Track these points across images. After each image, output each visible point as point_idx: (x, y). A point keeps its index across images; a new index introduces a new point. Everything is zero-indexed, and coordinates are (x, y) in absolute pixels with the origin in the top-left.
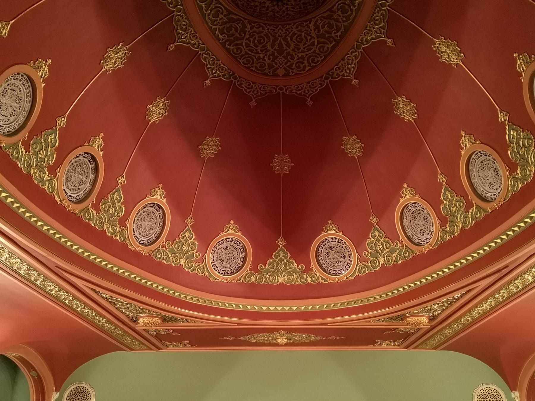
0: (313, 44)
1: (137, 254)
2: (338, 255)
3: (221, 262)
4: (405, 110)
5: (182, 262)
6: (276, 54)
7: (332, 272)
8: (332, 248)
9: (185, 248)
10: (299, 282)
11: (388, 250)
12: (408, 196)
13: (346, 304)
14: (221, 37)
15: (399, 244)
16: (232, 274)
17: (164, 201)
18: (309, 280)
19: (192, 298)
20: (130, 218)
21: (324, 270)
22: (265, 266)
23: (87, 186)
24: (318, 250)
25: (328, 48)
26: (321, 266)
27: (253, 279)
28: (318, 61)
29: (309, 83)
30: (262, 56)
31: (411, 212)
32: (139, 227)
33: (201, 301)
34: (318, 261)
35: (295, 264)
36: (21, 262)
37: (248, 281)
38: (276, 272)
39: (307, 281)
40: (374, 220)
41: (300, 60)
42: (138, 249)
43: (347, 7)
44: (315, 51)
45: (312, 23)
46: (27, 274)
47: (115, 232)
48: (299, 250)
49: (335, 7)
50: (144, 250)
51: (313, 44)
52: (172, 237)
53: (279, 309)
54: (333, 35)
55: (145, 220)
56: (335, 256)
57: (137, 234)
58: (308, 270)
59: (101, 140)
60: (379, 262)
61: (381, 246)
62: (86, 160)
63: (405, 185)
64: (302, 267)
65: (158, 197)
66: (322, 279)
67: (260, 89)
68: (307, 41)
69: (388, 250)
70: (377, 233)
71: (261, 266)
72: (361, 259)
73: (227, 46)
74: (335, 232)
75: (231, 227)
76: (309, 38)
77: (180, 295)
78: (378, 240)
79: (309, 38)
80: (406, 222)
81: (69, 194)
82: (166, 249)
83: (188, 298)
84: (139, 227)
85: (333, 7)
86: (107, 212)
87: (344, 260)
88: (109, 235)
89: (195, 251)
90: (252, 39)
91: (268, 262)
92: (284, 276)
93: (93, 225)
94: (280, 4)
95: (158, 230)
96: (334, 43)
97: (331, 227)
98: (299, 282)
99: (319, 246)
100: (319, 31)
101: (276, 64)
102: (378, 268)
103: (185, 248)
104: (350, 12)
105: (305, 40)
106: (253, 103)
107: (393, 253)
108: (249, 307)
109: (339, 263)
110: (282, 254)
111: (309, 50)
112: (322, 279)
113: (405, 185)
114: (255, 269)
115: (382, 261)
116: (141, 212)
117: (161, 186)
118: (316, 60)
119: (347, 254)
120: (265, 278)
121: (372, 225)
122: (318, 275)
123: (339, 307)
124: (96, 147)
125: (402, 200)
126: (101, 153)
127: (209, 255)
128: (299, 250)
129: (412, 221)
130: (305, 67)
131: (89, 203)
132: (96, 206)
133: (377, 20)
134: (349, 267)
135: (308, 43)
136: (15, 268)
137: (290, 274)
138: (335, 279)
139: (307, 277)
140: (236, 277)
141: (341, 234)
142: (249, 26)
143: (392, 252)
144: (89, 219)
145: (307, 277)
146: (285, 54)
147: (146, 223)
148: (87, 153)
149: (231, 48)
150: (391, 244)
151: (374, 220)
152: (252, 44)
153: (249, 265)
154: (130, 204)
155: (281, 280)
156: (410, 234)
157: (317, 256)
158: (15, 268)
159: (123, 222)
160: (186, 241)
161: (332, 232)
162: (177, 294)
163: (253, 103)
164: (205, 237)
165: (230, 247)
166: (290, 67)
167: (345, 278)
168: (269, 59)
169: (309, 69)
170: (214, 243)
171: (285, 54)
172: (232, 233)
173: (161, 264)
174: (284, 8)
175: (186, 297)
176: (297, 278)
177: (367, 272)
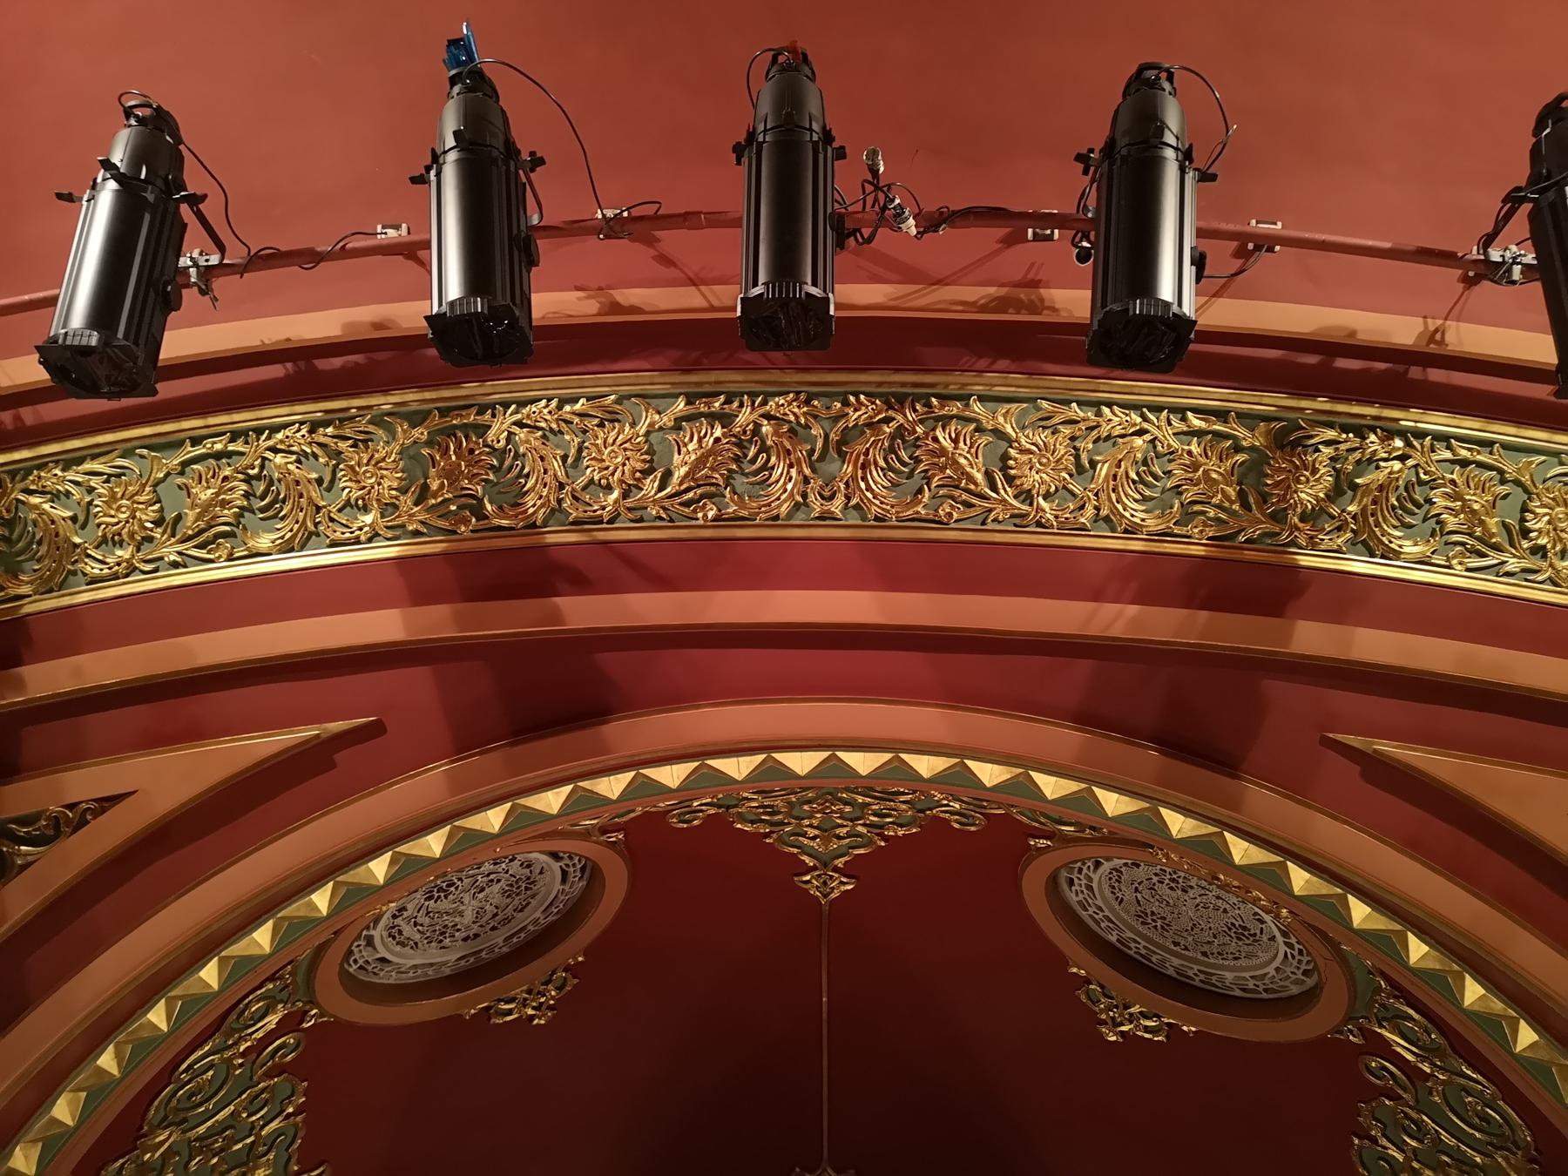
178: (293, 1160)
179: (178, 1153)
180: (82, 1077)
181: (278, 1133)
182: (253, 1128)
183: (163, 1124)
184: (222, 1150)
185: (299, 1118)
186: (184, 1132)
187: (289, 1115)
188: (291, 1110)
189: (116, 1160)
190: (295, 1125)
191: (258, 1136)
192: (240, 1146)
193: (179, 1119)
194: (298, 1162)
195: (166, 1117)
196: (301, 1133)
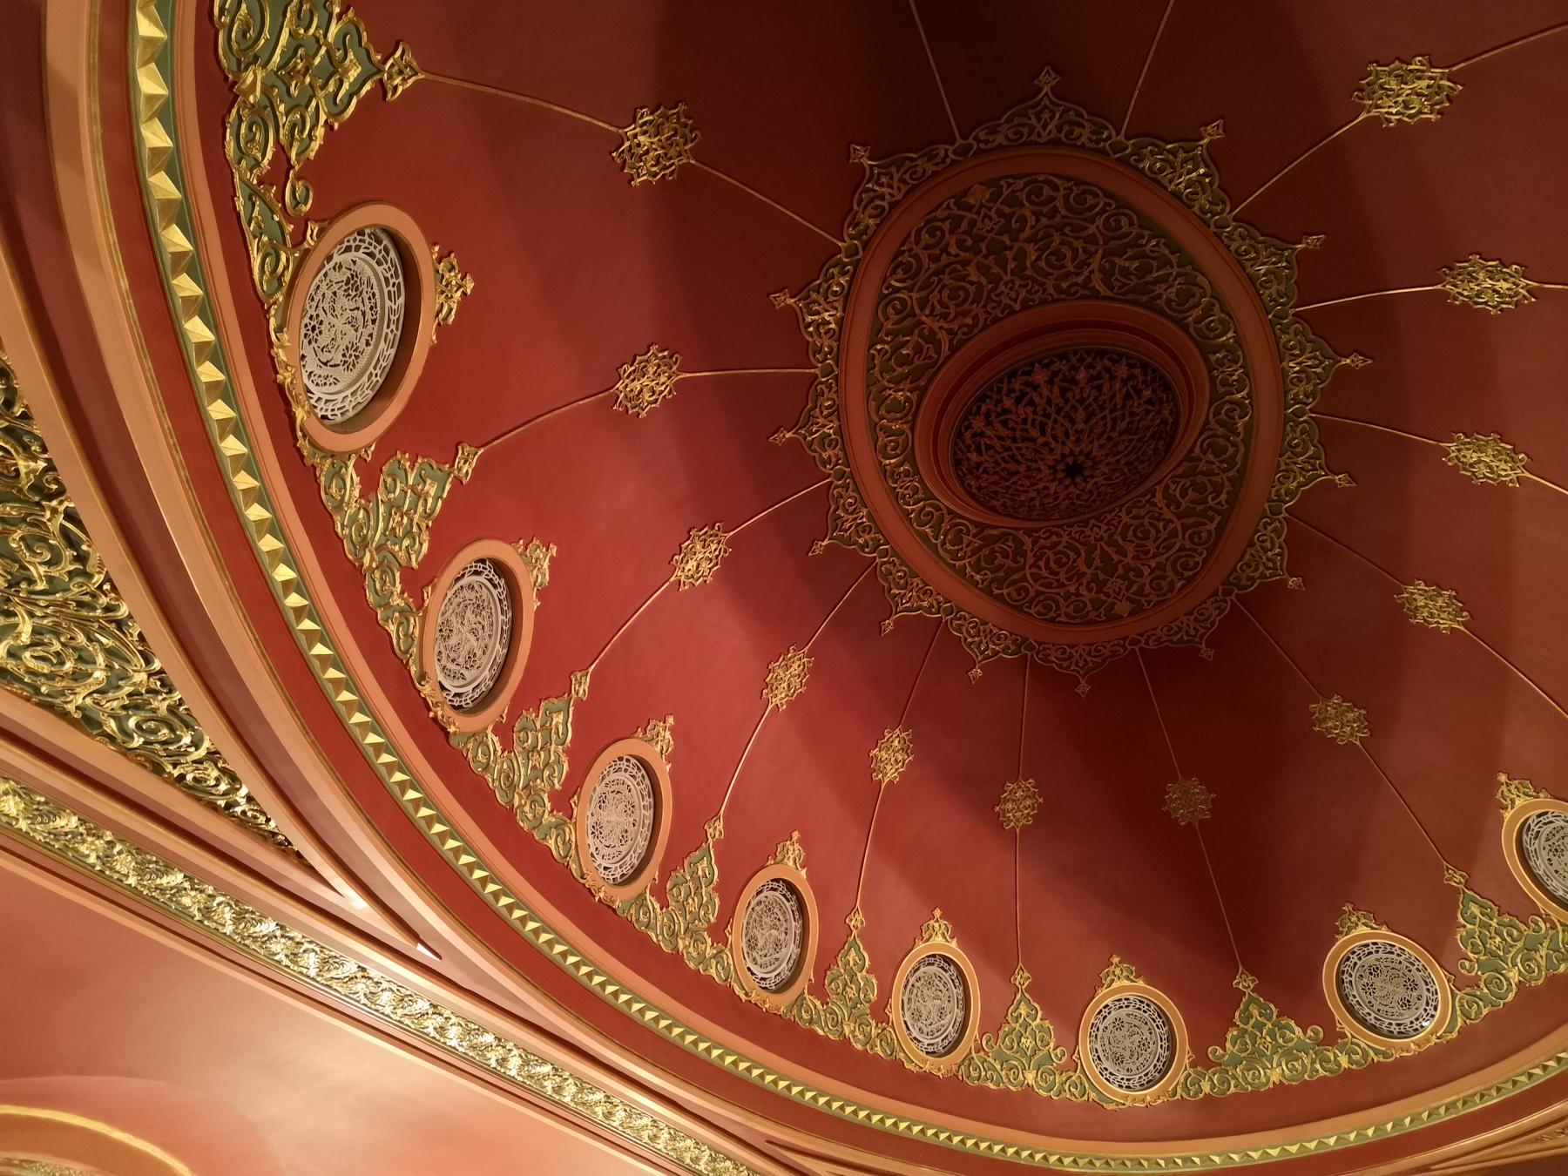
0: (1173, 534)
1: (927, 1078)
2: (1396, 986)
3: (1118, 1060)
4: (1434, 610)
5: (1030, 1077)
6: (1102, 577)
7: (1393, 1028)
8: (1374, 971)
9: (1027, 1042)
10: (1322, 1073)
11: (1520, 944)
12: (1519, 804)
13: (1460, 1105)
14: (978, 577)
15: (1542, 924)
16: (1151, 1083)
17: (954, 944)
18: (1344, 1061)
19: (1075, 1161)
20: (892, 1001)
21: (1373, 1028)
22: (1224, 1049)
23: (792, 950)
24: (1340, 982)
25: (1209, 532)
26: (1363, 1022)
27: (1206, 1087)
28: (1197, 564)
29: (1191, 613)
30: (1072, 589)
31: (1543, 837)
32: (917, 1015)
33: (1098, 1163)
34: (1351, 1009)
35: (1298, 1030)
36: (696, 1145)
37: (1196, 1094)
38: (1255, 1058)
39: (1339, 1065)
40: (1457, 879)
41: (1158, 573)
42: (927, 1068)
43: (1220, 441)
44: (1182, 548)
45: (1159, 495)
46: (714, 1170)
47: (868, 1039)
48: (1297, 993)
49: (1197, 450)
50: (940, 1067)
51: (1173, 534)
52: (994, 1023)
53: (1294, 1149)
54: (1211, 503)
55: (926, 996)
56: (1390, 987)
57: (915, 1033)
58: (1332, 1037)
59: (797, 846)
60: (1507, 979)
61: (1498, 939)
62: (777, 893)
63: (1503, 778)
64: (1317, 1034)
65: (939, 940)
66: (1377, 1052)
67: (1089, 654)
68: (1158, 531)
69: (1520, 944)
70: (1475, 909)
71: (1214, 1052)
72: (1460, 982)
73: (996, 592)
74: (1368, 930)
75: (1118, 971)
76: (1161, 525)
77: (1045, 1158)
78: (1487, 926)
79: (1161, 525)
80: (1540, 867)
81: (760, 975)
82: (987, 1053)
83: (1067, 1161)
84: (917, 1015)
85: (1191, 450)
86: (842, 995)
87: (1415, 994)
88: (859, 1047)
89: (1052, 1045)
90: (1042, 564)
91: (1229, 1036)
92: (1279, 1065)
93: (821, 1032)
94: (1078, 480)
95: (958, 1013)
96: (1218, 518)
97: (1354, 919)
98: (1322, 1073)
99: (1340, 973)
100: (1178, 505)
101: (1108, 595)
102: (1511, 996)
103: (1027, 1042)
104: (1231, 450)
105: (1153, 532)
106: (1083, 688)
107: (1536, 951)
108: (1216, 1159)
109: (1406, 1004)
110: (1255, 1012)
111: (1168, 548)
112: (1377, 1052)
113: (1503, 778)
114: (1202, 1061)
115: (1514, 976)
116: (912, 981)
117: (937, 913)
118: (1191, 563)
119: (1418, 977)
120: (1234, 1077)
121: (1456, 891)
122: (1361, 1047)
123: (1444, 1117)
124: (791, 863)
125: (1508, 815)
126: (803, 872)
127: (1085, 1047)
128: (1297, 993)
129: (1555, 860)
130: (1172, 583)
131: (802, 984)
132: (818, 990)
133: (1297, 445)
134: (1436, 1008)
135: (1163, 535)
136: (688, 1161)
137: (1290, 1056)
138: (1410, 1047)
139: (1336, 1056)
140: (1164, 1090)
141: (1384, 931)
142: (1028, 540)
143: (1531, 948)
144: (811, 1021)
145: (1336, 1056)
146: (1121, 570)
147: (929, 1004)
148: (777, 880)
149: (1005, 591)
150: (1523, 927)
151: (1457, 879)
152: (1045, 573)
153: (1184, 1054)
154: (885, 969)
155: (1275, 1076)
156: (1561, 893)
157: (1344, 998)
158: (688, 1161)
159: (880, 1011)
160: (1026, 1026)
161: (1360, 933)
162: (1038, 1157)
163: (1083, 688)
164: (1066, 1005)
165: (1129, 1020)
166: (1140, 592)
167: (1434, 1040)
168: (1090, 590)
169: (1183, 586)
170: (1089, 1017)
171: (1121, 570)
172: (1122, 987)
173: (983, 1091)
174: (1089, 486)
175: (1060, 1160)
176: (1313, 1062)
177: (1485, 1011)
178: (372, 51)
179: (274, 86)
180: (138, 53)
181: (342, 35)
182: (318, 40)
183: (241, 68)
184: (307, 69)
185: (351, 14)
186: (264, 66)
187: (340, 17)
188: (337, 10)
189: (229, 112)
190: (351, 21)
191: (327, 44)
192: (317, 60)
193: (249, 57)
194: (378, 52)
195: (239, 63)
196: (362, 27)
